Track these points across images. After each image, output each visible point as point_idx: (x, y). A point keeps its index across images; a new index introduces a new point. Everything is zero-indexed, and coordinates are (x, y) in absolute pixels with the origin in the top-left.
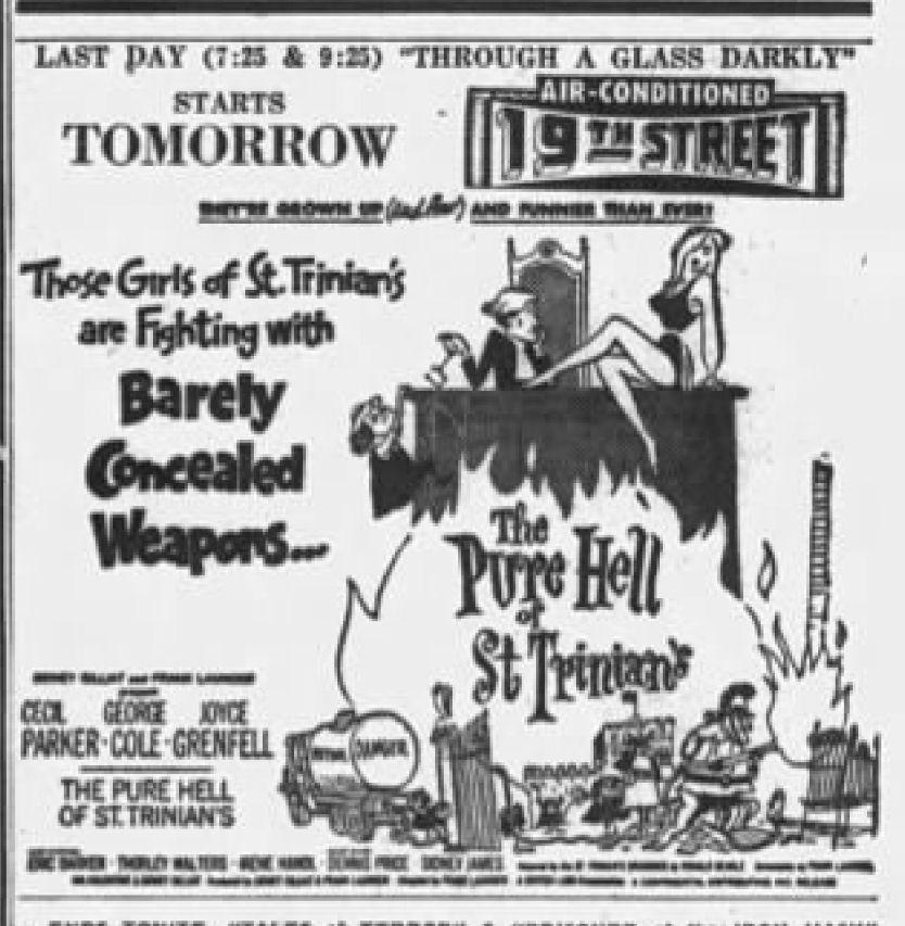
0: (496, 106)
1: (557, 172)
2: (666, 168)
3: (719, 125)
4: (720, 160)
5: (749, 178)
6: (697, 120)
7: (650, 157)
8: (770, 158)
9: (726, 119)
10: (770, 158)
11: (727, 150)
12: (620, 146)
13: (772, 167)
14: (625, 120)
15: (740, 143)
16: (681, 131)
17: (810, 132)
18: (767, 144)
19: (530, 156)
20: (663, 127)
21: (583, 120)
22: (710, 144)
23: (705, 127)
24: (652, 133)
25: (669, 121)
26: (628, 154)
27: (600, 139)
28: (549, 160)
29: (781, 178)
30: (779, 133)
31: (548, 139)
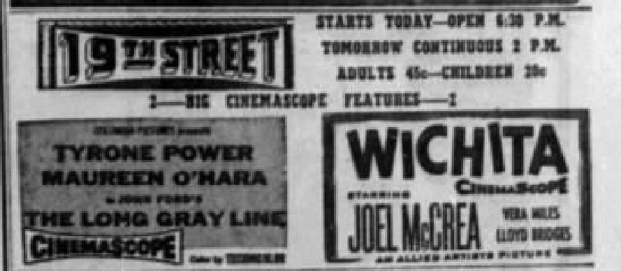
0: (59, 32)
1: (101, 76)
2: (180, 73)
3: (215, 42)
4: (216, 66)
5: (236, 78)
6: (200, 39)
7: (167, 65)
8: (252, 64)
9: (220, 38)
10: (252, 64)
11: (221, 59)
12: (147, 58)
13: (253, 71)
14: (149, 40)
15: (230, 54)
16: (189, 47)
17: (279, 45)
18: (248, 55)
19: (83, 65)
20: (176, 44)
21: (119, 41)
22: (209, 55)
23: (205, 42)
24: (169, 49)
25: (180, 40)
26: (151, 64)
27: (132, 54)
28: (96, 69)
29: (259, 79)
30: (257, 47)
31: (96, 54)
